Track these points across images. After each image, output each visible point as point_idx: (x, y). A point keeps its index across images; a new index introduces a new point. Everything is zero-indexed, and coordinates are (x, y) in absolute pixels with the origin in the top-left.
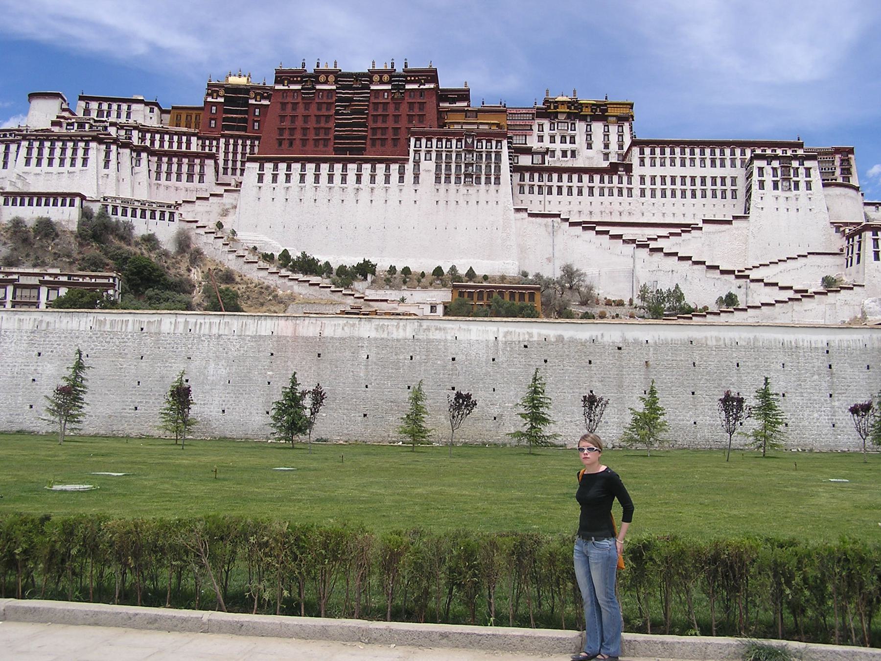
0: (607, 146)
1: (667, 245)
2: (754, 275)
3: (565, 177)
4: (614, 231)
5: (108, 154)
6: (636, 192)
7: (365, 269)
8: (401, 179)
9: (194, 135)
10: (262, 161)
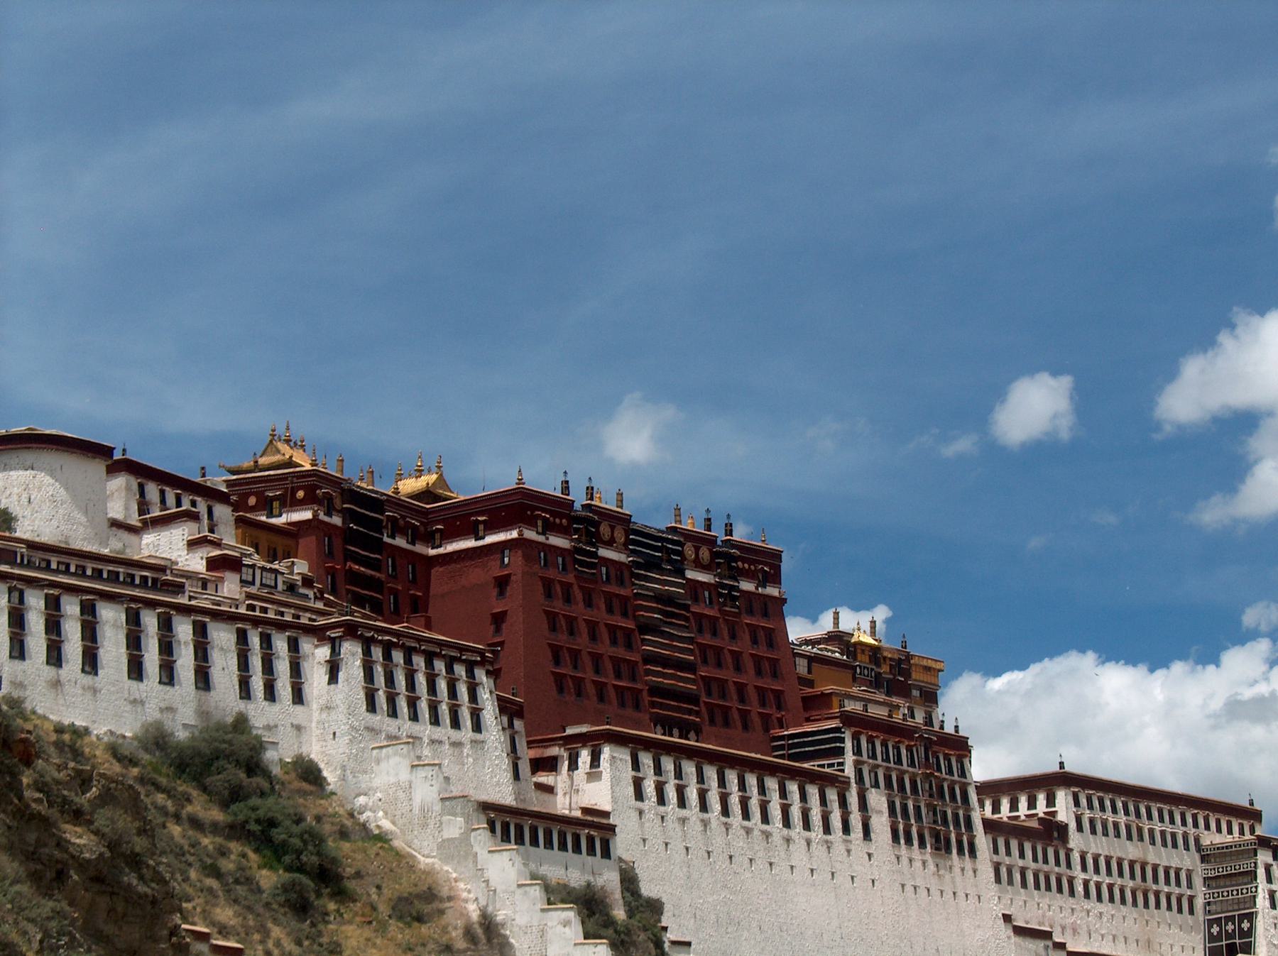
6: (1080, 889)
8: (846, 829)
10: (636, 745)
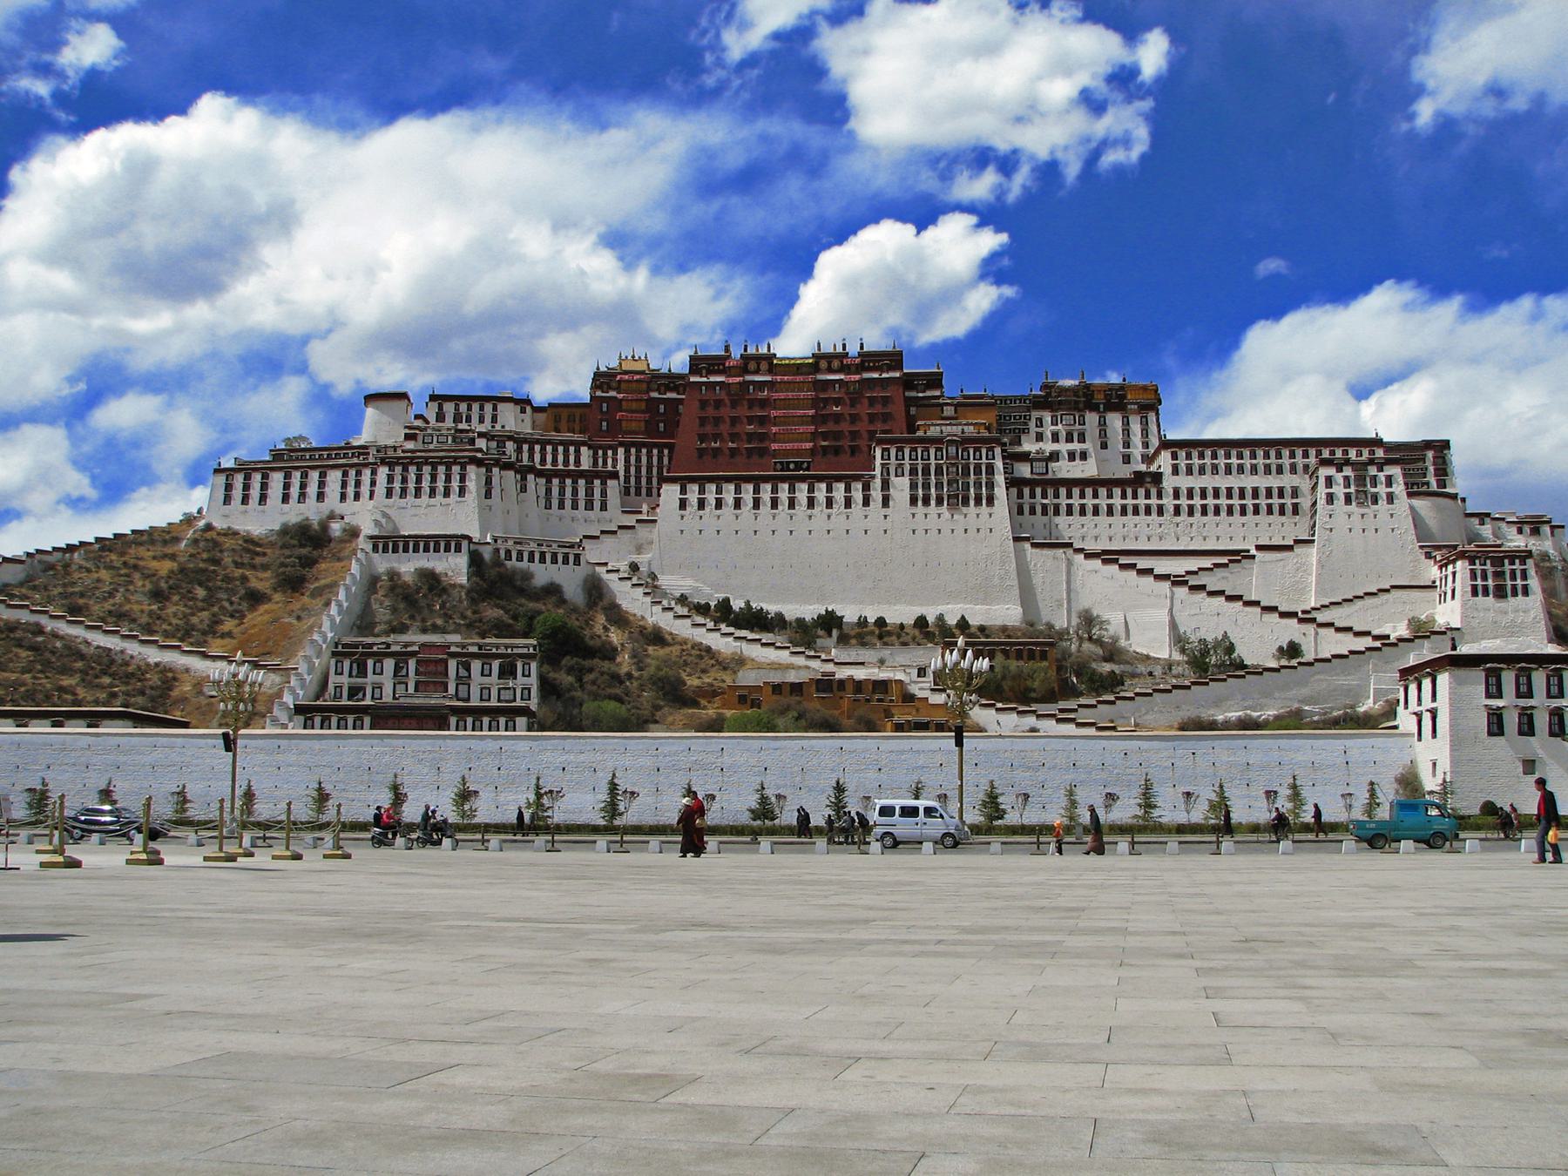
0: (1127, 445)
1: (1212, 582)
2: (1321, 617)
3: (1076, 491)
4: (1142, 563)
5: (489, 482)
7: (830, 622)
8: (866, 502)
9: (584, 443)
10: (684, 482)
